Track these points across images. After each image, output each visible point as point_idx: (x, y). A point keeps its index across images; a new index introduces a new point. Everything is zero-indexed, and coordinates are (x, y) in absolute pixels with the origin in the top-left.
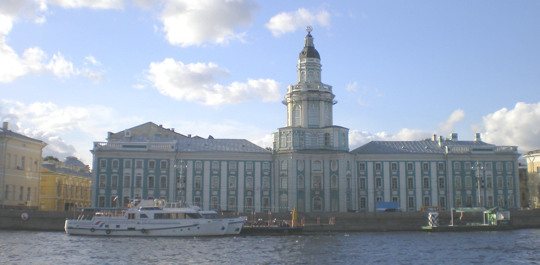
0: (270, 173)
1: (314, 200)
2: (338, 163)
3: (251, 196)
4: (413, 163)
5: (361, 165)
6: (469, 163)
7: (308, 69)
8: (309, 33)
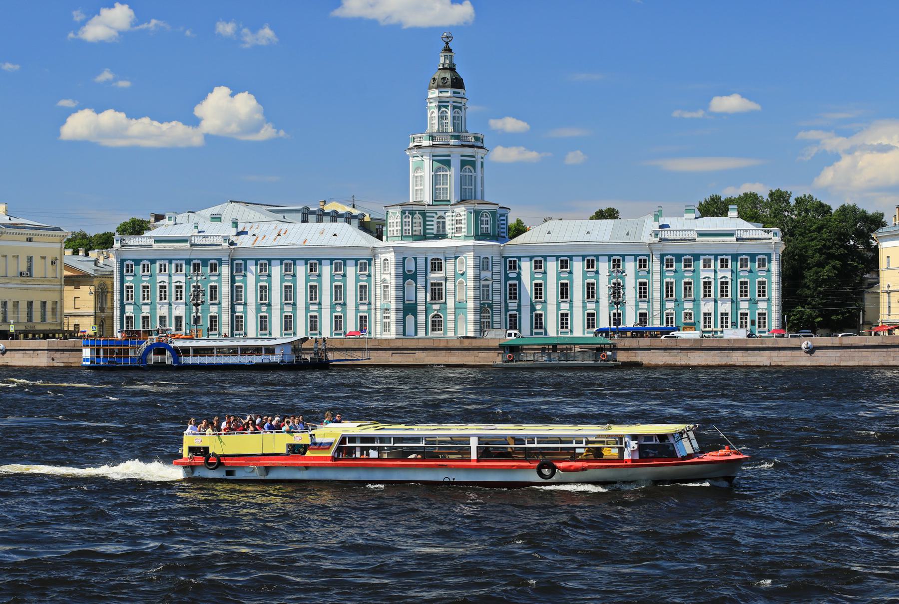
1: (433, 317)
2: (466, 261)
5: (510, 262)
6: (690, 257)
7: (439, 108)
8: (447, 43)
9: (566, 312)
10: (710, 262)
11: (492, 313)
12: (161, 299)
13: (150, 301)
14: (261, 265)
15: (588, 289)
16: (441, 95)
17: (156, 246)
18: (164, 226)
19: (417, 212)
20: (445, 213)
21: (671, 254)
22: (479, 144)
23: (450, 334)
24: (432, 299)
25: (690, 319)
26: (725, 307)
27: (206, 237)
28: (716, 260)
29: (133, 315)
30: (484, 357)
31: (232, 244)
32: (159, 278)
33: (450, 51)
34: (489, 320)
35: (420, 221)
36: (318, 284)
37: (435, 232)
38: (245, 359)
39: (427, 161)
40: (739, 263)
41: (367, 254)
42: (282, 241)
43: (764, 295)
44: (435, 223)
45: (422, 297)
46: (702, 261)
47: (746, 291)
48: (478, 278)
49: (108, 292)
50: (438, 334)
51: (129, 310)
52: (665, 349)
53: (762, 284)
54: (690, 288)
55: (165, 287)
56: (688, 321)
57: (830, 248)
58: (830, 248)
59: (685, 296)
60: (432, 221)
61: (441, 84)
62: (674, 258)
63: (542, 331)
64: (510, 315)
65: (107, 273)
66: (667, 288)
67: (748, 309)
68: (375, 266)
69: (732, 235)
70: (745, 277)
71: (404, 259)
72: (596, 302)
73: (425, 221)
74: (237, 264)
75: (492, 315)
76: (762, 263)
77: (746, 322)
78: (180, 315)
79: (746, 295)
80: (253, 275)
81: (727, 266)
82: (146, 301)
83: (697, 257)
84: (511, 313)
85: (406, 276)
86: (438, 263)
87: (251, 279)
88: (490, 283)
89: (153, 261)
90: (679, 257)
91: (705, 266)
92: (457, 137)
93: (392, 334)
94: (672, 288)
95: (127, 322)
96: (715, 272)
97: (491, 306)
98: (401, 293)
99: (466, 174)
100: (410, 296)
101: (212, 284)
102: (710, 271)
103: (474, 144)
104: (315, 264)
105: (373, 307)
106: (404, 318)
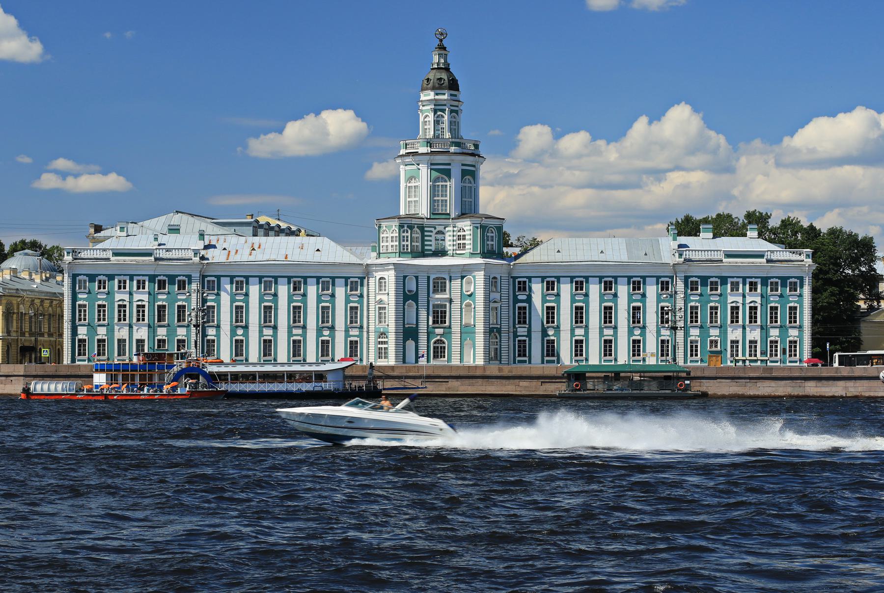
1: (435, 343)
3: (329, 336)
4: (613, 280)
5: (519, 283)
6: (717, 280)
7: (435, 111)
8: (441, 40)
9: (581, 338)
10: (739, 285)
11: (501, 338)
12: (119, 320)
13: (106, 322)
14: (237, 282)
15: (605, 313)
16: (437, 97)
17: (114, 259)
18: (115, 238)
19: (416, 226)
20: (445, 228)
21: (696, 277)
22: (476, 152)
23: (456, 362)
24: (434, 322)
25: (716, 346)
26: (754, 334)
27: (168, 250)
28: (744, 284)
29: (87, 338)
30: (526, 387)
31: (203, 258)
32: (118, 297)
33: (445, 49)
34: (497, 347)
35: (418, 235)
36: (302, 305)
37: (433, 248)
38: (293, 386)
39: (424, 171)
40: (769, 287)
41: (358, 272)
42: (259, 257)
43: (795, 322)
44: (433, 239)
45: (425, 320)
46: (729, 285)
47: (776, 317)
48: (488, 300)
49: (14, 313)
50: (441, 362)
51: (82, 332)
52: (733, 378)
53: (793, 309)
54: (716, 313)
55: (125, 306)
56: (714, 349)
57: (827, 273)
58: (827, 273)
59: (711, 322)
60: (431, 236)
61: (437, 85)
62: (699, 280)
63: (555, 359)
64: (519, 341)
65: (12, 291)
66: (692, 313)
67: (778, 337)
68: (368, 285)
69: (762, 256)
70: (776, 302)
71: (405, 277)
72: (614, 328)
73: (423, 236)
74: (208, 281)
75: (500, 341)
76: (793, 288)
77: (776, 351)
78: (143, 338)
79: (776, 322)
80: (228, 294)
81: (756, 290)
82: (102, 322)
83: (724, 280)
84: (520, 338)
85: (406, 296)
86: (441, 283)
87: (225, 298)
88: (498, 305)
89: (111, 277)
90: (704, 280)
91: (732, 290)
92: (458, 144)
93: (391, 361)
94: (696, 313)
95: (79, 346)
96: (744, 296)
97: (499, 331)
98: (401, 315)
99: (464, 185)
100: (411, 319)
101: (180, 303)
102: (738, 295)
103: (473, 152)
104: (299, 282)
105: (365, 329)
106: (404, 342)
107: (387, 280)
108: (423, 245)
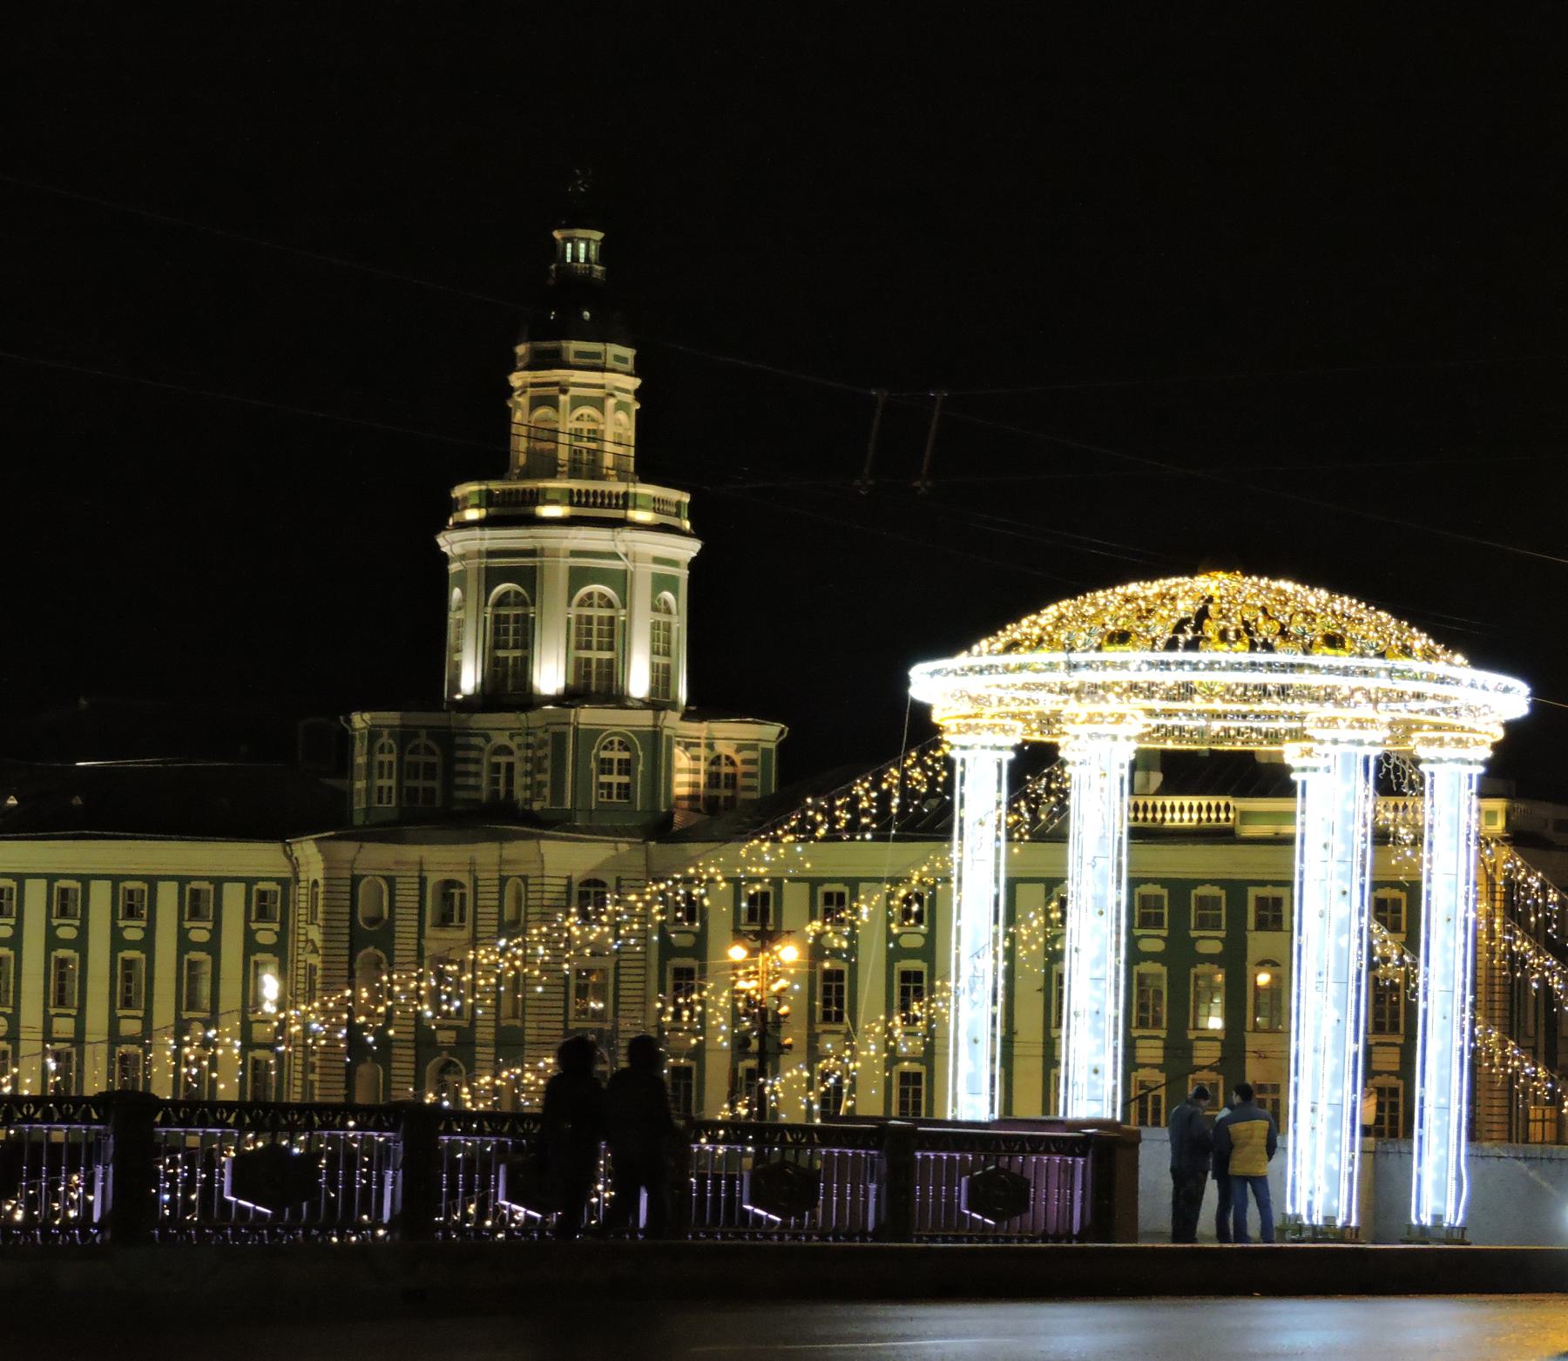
0: (282, 935)
6: (1215, 891)
19: (423, 733)
60: (478, 761)
62: (1165, 892)
71: (355, 881)
99: (586, 611)
107: (469, 892)
108: (449, 787)
